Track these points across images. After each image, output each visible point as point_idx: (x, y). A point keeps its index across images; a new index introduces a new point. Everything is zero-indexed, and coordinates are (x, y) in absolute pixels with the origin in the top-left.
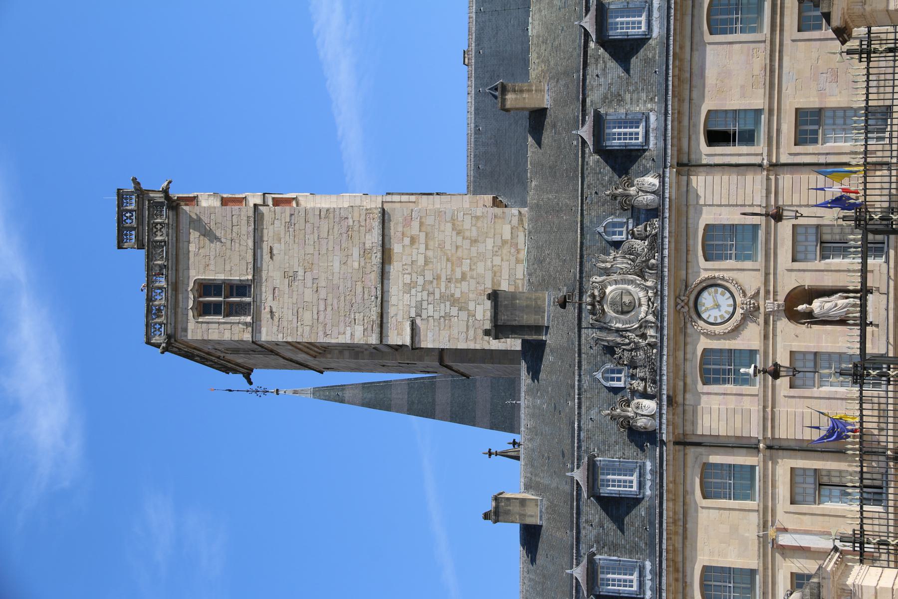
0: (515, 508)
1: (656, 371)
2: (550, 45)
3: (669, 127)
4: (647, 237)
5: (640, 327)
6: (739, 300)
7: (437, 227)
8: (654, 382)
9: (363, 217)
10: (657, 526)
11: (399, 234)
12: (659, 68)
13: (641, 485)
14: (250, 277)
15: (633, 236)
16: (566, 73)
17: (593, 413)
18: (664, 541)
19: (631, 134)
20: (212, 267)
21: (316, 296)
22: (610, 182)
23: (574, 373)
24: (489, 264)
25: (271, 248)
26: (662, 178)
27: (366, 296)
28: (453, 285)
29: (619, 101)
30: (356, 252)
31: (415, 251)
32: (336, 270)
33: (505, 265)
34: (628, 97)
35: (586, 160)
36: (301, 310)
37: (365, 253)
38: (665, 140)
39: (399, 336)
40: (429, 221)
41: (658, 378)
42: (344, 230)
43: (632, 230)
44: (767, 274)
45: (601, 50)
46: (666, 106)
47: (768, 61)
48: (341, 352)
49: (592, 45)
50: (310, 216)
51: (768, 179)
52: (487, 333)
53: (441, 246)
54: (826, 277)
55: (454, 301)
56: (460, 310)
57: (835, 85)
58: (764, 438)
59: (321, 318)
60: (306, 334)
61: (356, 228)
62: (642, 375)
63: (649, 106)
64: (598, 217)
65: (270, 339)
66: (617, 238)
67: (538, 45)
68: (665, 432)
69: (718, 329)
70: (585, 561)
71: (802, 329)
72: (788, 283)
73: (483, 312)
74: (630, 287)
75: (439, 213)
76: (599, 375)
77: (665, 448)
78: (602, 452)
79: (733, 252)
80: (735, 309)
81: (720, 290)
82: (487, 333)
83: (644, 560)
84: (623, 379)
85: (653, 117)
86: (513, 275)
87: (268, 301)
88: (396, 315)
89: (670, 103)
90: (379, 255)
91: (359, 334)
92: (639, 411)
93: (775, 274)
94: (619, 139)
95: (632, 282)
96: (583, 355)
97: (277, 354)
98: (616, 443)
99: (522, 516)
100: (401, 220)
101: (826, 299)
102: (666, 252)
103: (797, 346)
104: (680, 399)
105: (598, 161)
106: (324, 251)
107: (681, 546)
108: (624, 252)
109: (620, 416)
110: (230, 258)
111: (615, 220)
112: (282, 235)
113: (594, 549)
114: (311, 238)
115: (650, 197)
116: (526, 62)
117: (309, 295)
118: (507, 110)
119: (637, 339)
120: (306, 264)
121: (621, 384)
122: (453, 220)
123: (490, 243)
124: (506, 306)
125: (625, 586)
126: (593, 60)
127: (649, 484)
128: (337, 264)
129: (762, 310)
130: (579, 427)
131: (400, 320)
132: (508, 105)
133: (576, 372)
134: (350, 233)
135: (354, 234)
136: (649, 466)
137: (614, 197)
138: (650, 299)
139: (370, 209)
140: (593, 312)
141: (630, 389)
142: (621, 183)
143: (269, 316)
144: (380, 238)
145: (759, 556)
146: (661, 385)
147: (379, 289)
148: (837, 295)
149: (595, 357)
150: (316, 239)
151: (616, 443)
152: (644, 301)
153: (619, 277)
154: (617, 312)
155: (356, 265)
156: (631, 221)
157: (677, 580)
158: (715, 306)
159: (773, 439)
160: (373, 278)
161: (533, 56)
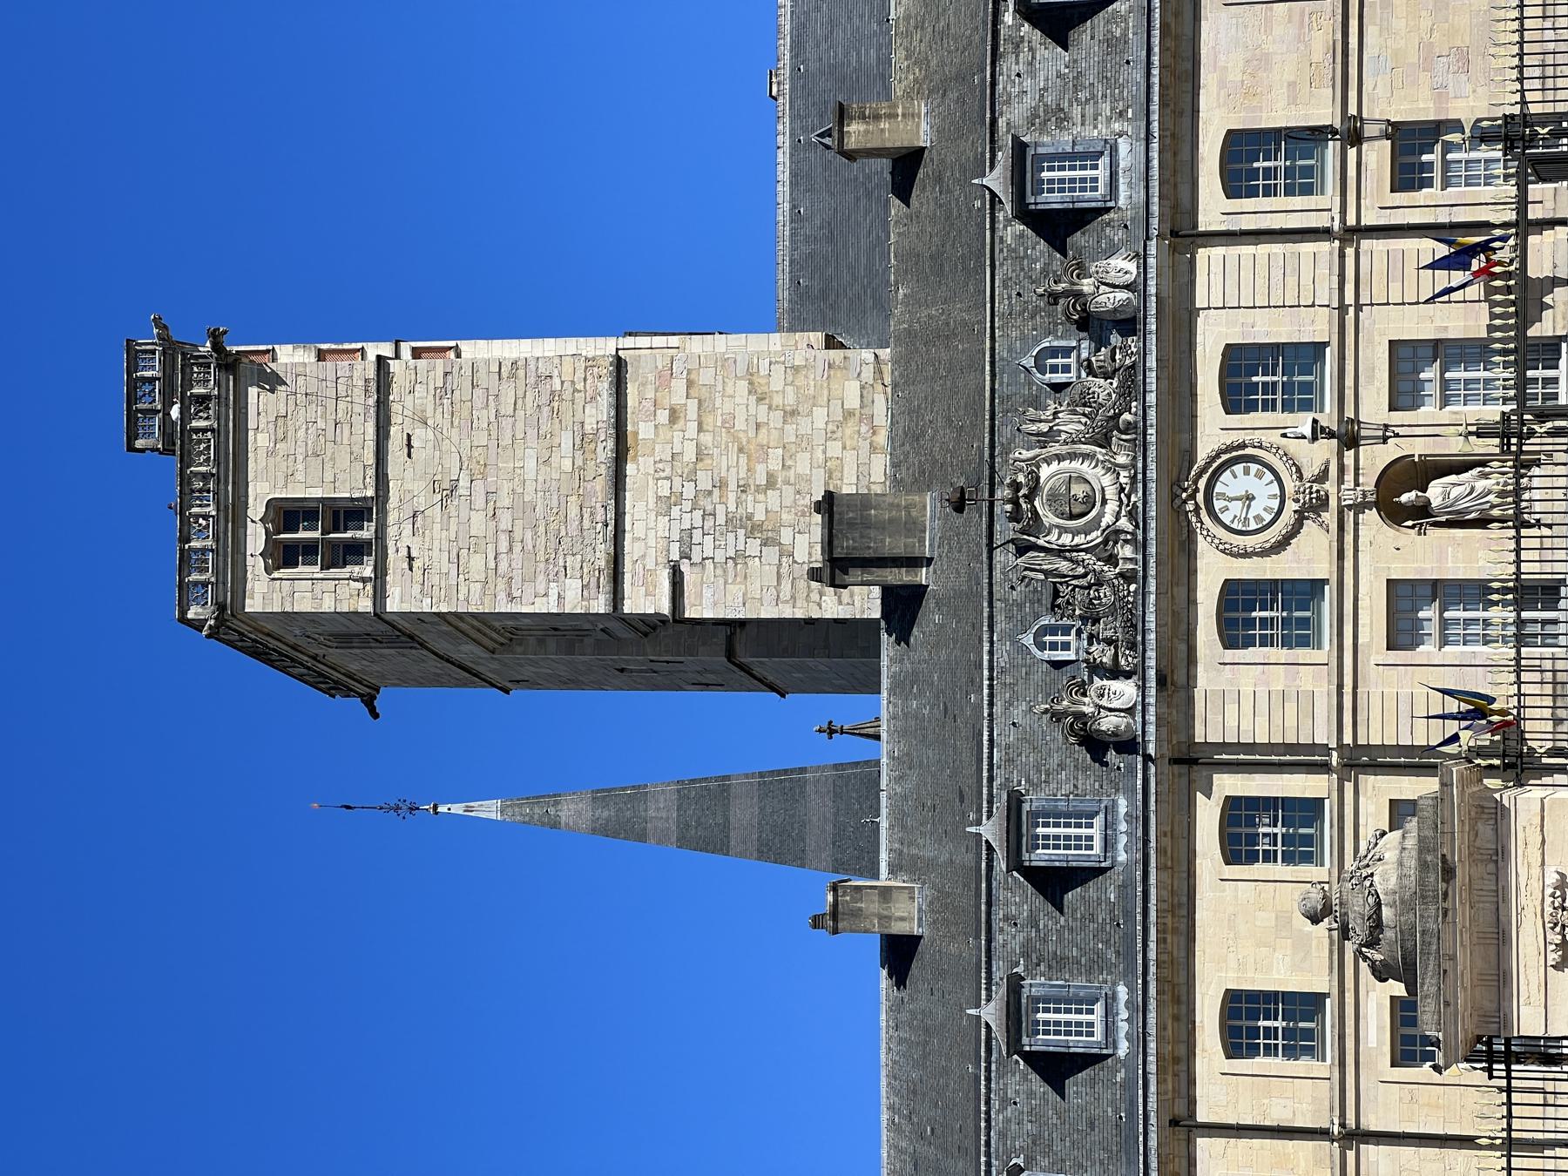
0: (871, 905)
1: (1134, 626)
2: (930, 30)
3: (1155, 163)
4: (1116, 370)
5: (1105, 542)
6: (1290, 486)
7: (720, 388)
8: (1132, 646)
9: (580, 374)
10: (1139, 917)
11: (649, 405)
12: (1137, 52)
13: (1108, 844)
14: (370, 493)
15: (1091, 371)
16: (961, 78)
17: (1018, 713)
18: (1152, 946)
19: (1083, 180)
20: (300, 476)
21: (492, 524)
22: (1045, 272)
23: (981, 640)
24: (819, 455)
25: (409, 436)
26: (1142, 258)
27: (586, 524)
28: (750, 498)
29: (1060, 121)
30: (566, 440)
31: (678, 436)
32: (530, 474)
33: (850, 457)
34: (1076, 111)
35: (999, 233)
36: (464, 552)
37: (584, 441)
38: (1147, 187)
39: (646, 597)
40: (705, 377)
41: (1139, 638)
42: (545, 399)
43: (1088, 360)
45: (1026, 27)
46: (1148, 123)
47: (1339, 36)
48: (541, 641)
49: (1008, 18)
50: (482, 377)
51: (1342, 256)
52: (814, 575)
53: (728, 424)
55: (754, 529)
56: (764, 544)
57: (1464, 77)
58: (1341, 746)
59: (503, 566)
60: (475, 598)
61: (567, 395)
62: (1109, 634)
63: (1117, 126)
64: (1023, 338)
65: (406, 608)
66: (1060, 378)
67: (908, 34)
68: (1153, 738)
69: (1250, 542)
70: (1000, 992)
71: (1407, 536)
73: (808, 546)
74: (1085, 468)
75: (723, 362)
76: (1028, 640)
77: (1153, 769)
78: (1035, 786)
79: (1279, 397)
80: (1282, 503)
81: (1254, 467)
82: (814, 575)
83: (1114, 984)
84: (1073, 646)
85: (1123, 147)
86: (864, 469)
87: (399, 537)
88: (644, 556)
89: (1155, 117)
90: (611, 444)
91: (572, 594)
92: (1104, 702)
94: (1061, 190)
95: (1086, 456)
96: (998, 604)
97: (423, 645)
98: (1062, 766)
99: (885, 919)
100: (651, 377)
102: (1152, 398)
104: (1180, 677)
105: (1022, 235)
106: (507, 441)
107: (1183, 954)
108: (1073, 403)
109: (1065, 714)
110: (333, 459)
111: (1055, 344)
112: (429, 413)
113: (1020, 970)
114: (484, 416)
115: (1122, 295)
116: (884, 78)
117: (478, 523)
118: (851, 156)
119: (1099, 565)
120: (473, 466)
121: (1070, 655)
122: (750, 375)
123: (820, 414)
124: (851, 524)
125: (1079, 1034)
126: (1010, 47)
127: (1123, 840)
128: (531, 464)
129: (1333, 502)
130: (991, 740)
131: (650, 565)
132: (851, 143)
133: (986, 636)
134: (556, 404)
135: (566, 406)
136: (1123, 805)
137: (1054, 298)
138: (1122, 490)
139: (594, 359)
140: (1015, 516)
141: (1086, 661)
142: (1066, 270)
143: (406, 565)
144: (613, 413)
145: (1331, 969)
146: (1144, 651)
147: (611, 507)
148: (1475, 472)
149: (1021, 606)
150: (492, 419)
151: (1062, 766)
152: (1111, 493)
153: (1065, 449)
154: (1061, 515)
155: (567, 465)
156: (1085, 344)
157: (1176, 1018)
158: (1246, 495)
159: (1356, 745)
160: (600, 487)
161: (898, 57)
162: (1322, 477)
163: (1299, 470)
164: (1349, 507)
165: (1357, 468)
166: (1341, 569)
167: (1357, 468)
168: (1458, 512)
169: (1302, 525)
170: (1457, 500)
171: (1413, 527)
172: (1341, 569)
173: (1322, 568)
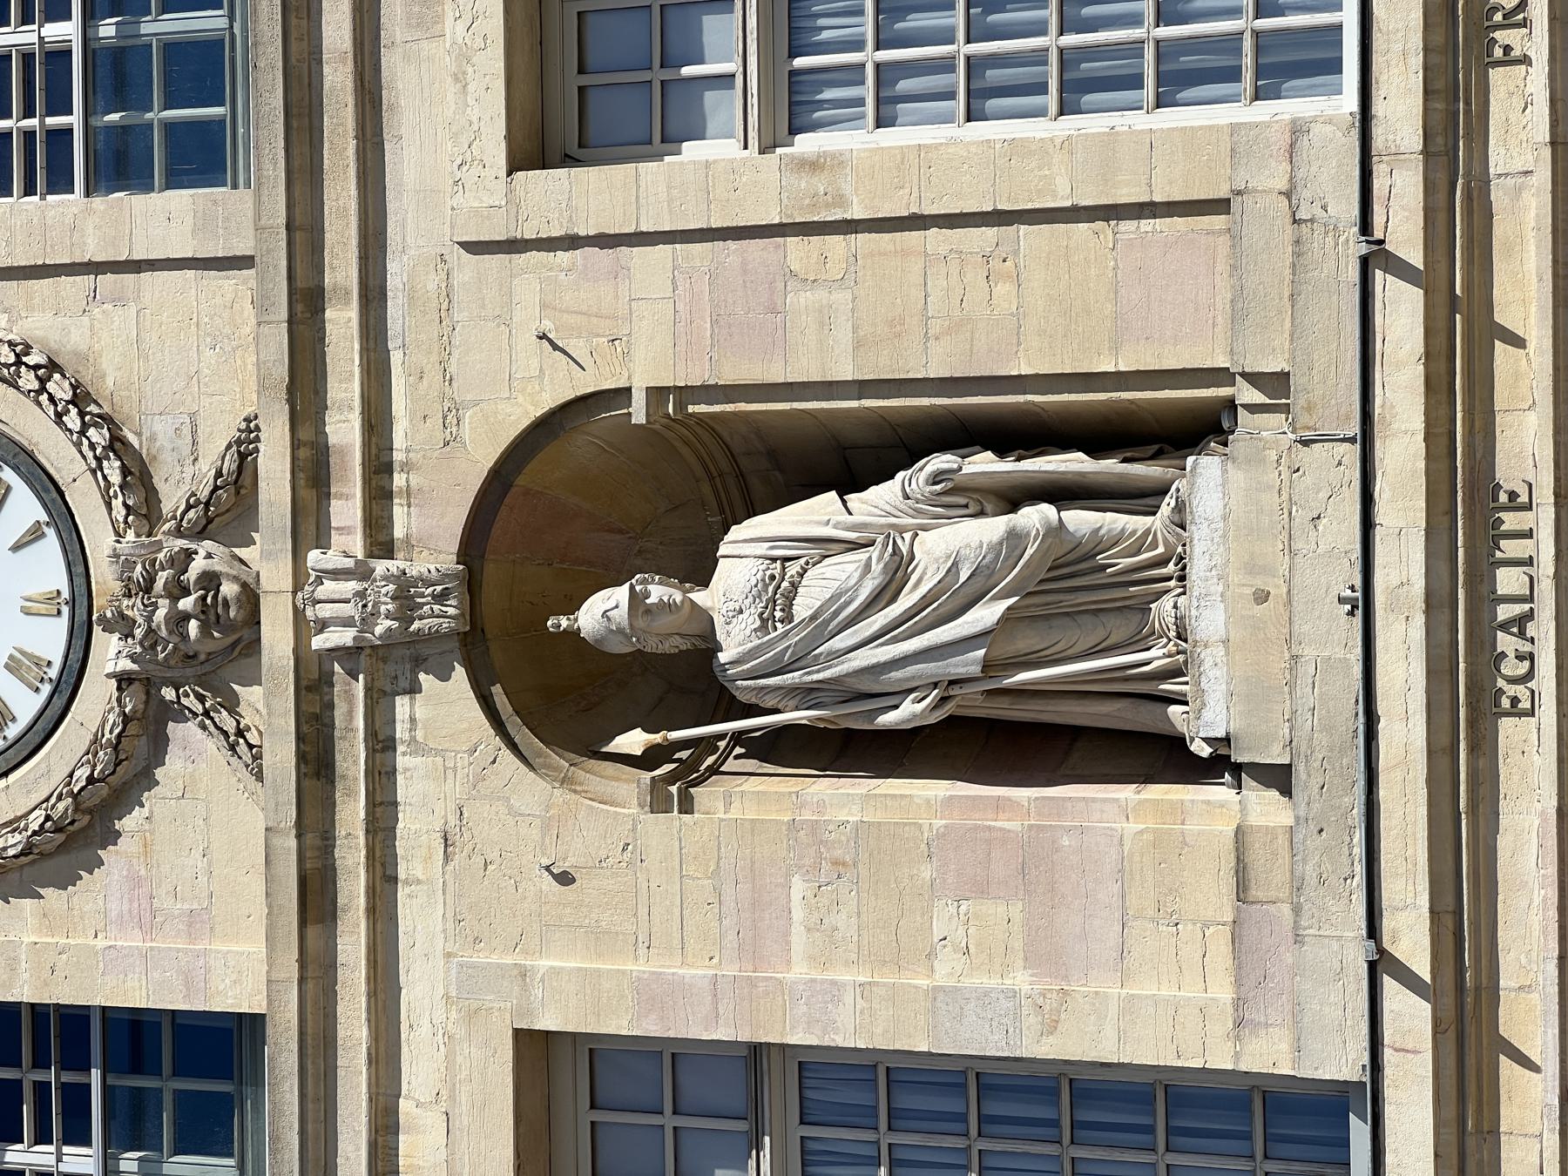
44: (307, 304)
54: (801, 300)
71: (603, 809)
72: (483, 364)
93: (373, 296)
103: (602, 988)
148: (918, 477)
162: (229, 507)
163: (138, 476)
164: (349, 655)
165: (378, 467)
166: (317, 972)
167: (378, 467)
168: (848, 692)
169: (158, 747)
170: (824, 625)
171: (648, 759)
172: (317, 972)
173: (235, 970)
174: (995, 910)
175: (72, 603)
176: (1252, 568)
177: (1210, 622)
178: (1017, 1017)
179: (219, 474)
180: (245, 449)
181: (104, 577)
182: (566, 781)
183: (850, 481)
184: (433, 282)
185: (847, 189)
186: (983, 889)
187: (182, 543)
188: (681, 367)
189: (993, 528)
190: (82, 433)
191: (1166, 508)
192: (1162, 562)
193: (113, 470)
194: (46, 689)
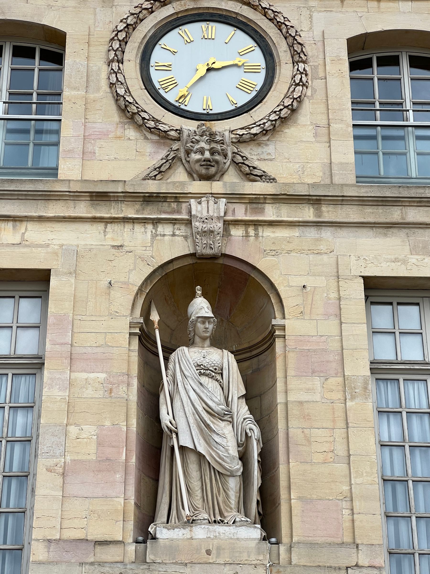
44: (315, 201)
101: (237, 388)
174: (92, 448)
175: (208, 114)
176: (219, 549)
177: (200, 532)
178: (53, 456)
179: (254, 168)
180: (263, 177)
181: (219, 127)
182: (140, 290)
183: (248, 398)
184: (323, 247)
185: (357, 400)
186: (99, 444)
187: (230, 155)
188: (293, 338)
189: (234, 451)
190: (269, 120)
191: (241, 517)
192: (221, 514)
193: (255, 130)
194: (177, 104)
